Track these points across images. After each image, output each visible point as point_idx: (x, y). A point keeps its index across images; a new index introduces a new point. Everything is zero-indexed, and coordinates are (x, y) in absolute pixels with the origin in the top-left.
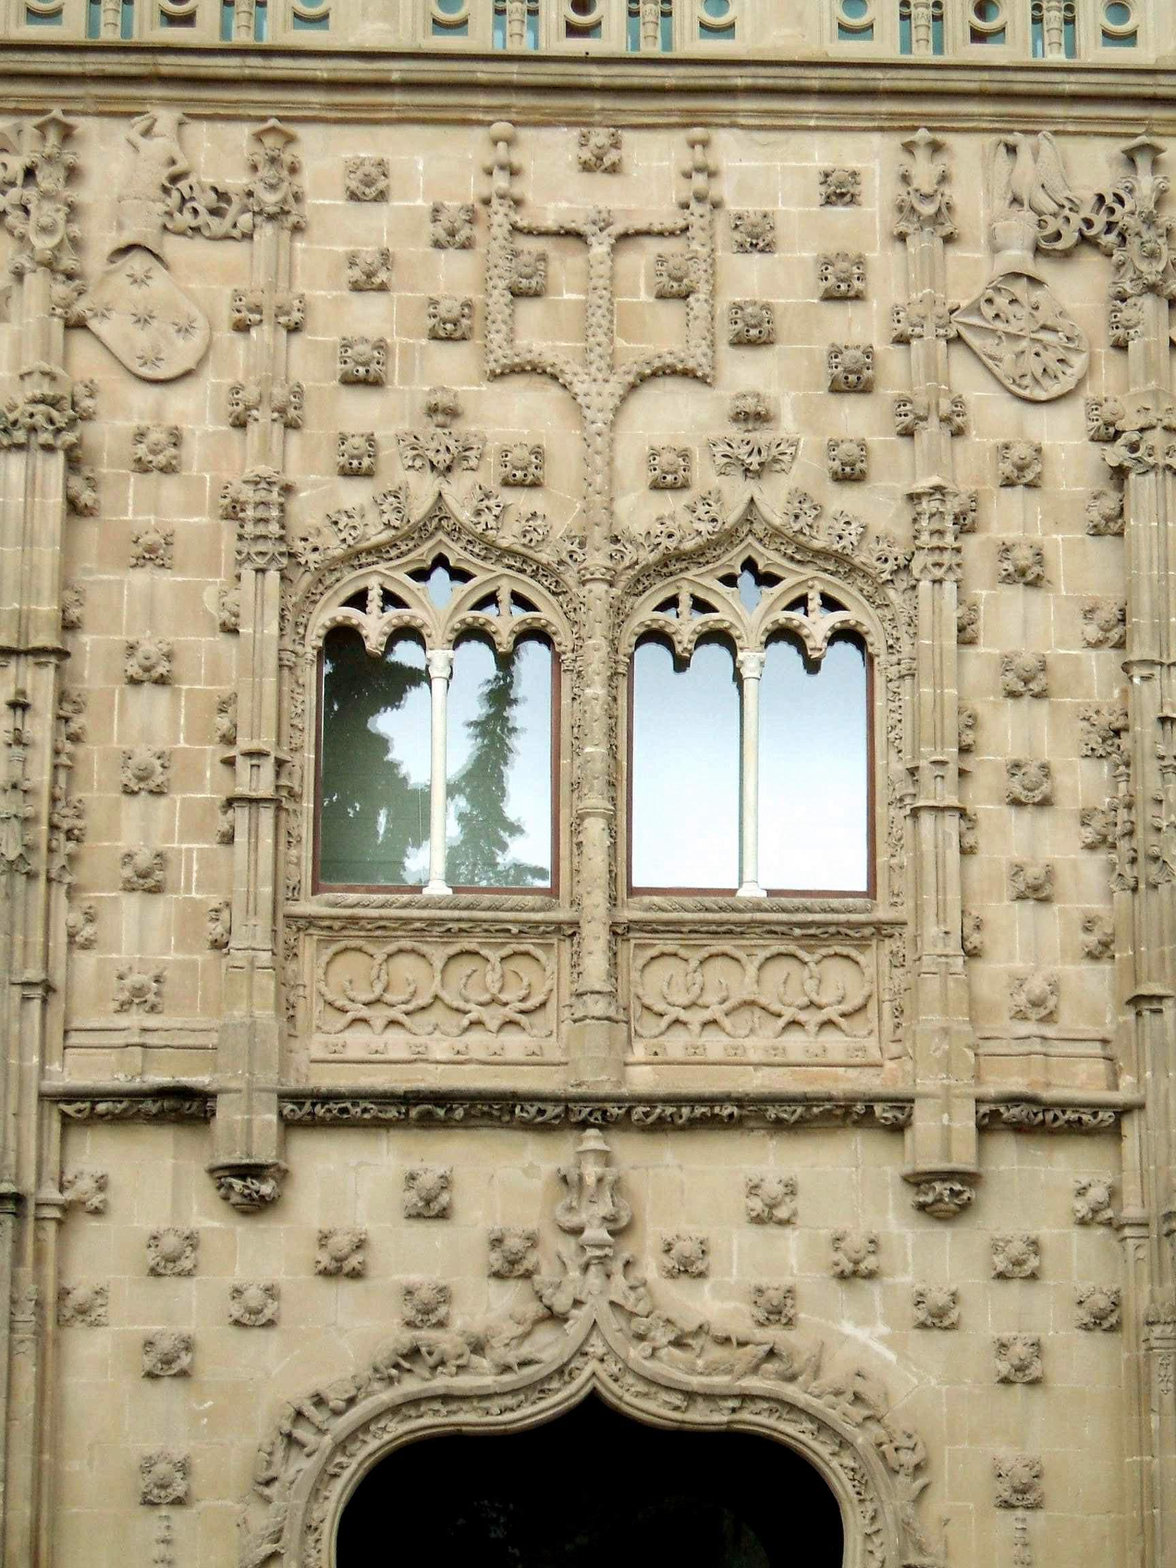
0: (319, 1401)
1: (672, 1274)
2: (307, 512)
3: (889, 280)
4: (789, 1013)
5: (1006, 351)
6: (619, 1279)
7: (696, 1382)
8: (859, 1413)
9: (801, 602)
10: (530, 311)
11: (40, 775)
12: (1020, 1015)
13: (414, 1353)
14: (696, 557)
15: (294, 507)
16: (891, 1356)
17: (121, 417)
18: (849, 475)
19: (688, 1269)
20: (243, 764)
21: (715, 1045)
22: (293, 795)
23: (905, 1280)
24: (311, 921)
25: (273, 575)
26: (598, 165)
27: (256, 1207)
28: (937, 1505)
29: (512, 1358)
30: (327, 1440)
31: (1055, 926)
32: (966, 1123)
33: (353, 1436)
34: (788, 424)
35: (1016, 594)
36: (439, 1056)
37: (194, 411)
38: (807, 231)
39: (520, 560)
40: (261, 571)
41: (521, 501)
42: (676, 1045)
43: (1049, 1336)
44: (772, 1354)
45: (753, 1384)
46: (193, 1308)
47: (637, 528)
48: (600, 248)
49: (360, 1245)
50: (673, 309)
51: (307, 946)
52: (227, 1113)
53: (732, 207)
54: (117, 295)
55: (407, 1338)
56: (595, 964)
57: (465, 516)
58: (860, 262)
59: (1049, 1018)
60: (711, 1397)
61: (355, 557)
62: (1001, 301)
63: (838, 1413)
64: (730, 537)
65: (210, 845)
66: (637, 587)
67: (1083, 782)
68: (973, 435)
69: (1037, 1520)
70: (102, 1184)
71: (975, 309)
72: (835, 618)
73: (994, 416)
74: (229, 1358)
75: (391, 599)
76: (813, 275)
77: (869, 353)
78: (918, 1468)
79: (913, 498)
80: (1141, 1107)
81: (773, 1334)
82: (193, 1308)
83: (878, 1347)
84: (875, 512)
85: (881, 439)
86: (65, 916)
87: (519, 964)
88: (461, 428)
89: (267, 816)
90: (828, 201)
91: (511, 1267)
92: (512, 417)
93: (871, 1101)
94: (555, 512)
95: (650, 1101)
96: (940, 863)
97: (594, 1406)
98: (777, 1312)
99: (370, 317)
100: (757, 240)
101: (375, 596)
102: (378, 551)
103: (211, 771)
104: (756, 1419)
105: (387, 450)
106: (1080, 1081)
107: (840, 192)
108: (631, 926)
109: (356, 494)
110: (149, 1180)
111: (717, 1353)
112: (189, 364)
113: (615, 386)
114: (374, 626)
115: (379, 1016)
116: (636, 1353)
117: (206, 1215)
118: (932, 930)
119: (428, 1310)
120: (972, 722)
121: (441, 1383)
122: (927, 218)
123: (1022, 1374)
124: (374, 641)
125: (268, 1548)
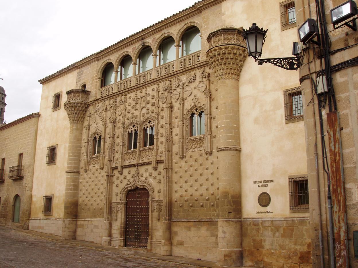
2: (126, 123)
3: (156, 97)
10: (137, 105)
11: (111, 146)
16: (152, 181)
17: (118, 118)
24: (125, 153)
26: (141, 92)
27: (121, 174)
28: (155, 193)
31: (163, 146)
34: (150, 110)
35: (162, 119)
37: (121, 117)
45: (144, 184)
48: (140, 99)
51: (126, 156)
54: (118, 110)
56: (137, 153)
59: (162, 153)
63: (148, 186)
64: (147, 119)
69: (160, 194)
70: (115, 173)
78: (153, 190)
85: (155, 109)
86: (113, 155)
92: (136, 113)
98: (146, 178)
99: (130, 108)
100: (149, 96)
104: (145, 187)
106: (163, 158)
107: (153, 90)
108: (141, 151)
112: (120, 114)
116: (137, 183)
117: (119, 175)
118: (154, 148)
119: (129, 181)
120: (159, 130)
122: (158, 91)
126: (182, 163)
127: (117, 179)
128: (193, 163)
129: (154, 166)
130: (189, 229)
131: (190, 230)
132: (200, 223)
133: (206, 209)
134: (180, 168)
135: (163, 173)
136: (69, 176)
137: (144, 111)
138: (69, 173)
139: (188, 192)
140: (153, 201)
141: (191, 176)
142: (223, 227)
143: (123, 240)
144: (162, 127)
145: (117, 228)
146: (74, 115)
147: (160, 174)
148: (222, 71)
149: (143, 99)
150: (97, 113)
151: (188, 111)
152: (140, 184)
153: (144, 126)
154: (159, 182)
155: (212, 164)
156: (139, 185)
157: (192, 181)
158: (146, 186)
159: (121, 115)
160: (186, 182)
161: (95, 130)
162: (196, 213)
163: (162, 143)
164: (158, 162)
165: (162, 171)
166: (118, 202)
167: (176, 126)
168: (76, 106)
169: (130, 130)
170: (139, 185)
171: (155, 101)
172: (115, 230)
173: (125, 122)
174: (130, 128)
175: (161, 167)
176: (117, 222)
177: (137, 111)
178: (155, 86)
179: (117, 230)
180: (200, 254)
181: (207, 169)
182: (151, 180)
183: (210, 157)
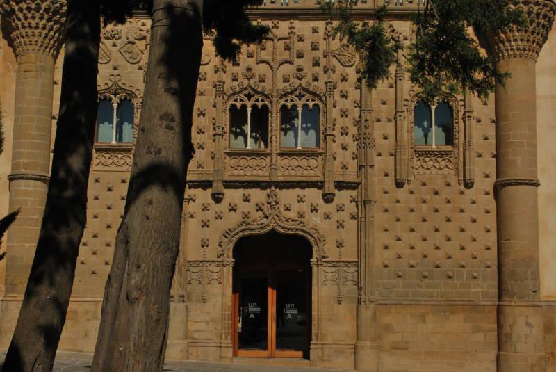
0: (230, 230)
1: (285, 210)
3: (322, 46)
4: (305, 168)
5: (342, 57)
6: (277, 211)
7: (289, 227)
8: (315, 231)
9: (308, 100)
12: (342, 168)
13: (244, 222)
14: (292, 93)
15: (225, 86)
18: (316, 79)
19: (288, 209)
20: (217, 129)
21: (293, 173)
22: (225, 133)
23: (323, 211)
25: (222, 97)
29: (259, 223)
30: (230, 236)
31: (348, 153)
32: (332, 186)
33: (235, 235)
34: (306, 70)
36: (249, 175)
38: (309, 38)
39: (262, 94)
40: (219, 96)
41: (263, 84)
42: (286, 173)
43: (345, 220)
44: (301, 222)
45: (298, 227)
46: (209, 215)
47: (281, 88)
48: (276, 41)
49: (236, 205)
50: (287, 52)
52: (215, 184)
53: (297, 33)
55: (243, 220)
57: (253, 86)
58: (318, 43)
60: (292, 230)
61: (235, 94)
62: (342, 49)
64: (296, 90)
65: (212, 141)
66: (281, 98)
67: (353, 130)
68: (337, 72)
69: (342, 249)
71: (337, 50)
72: (314, 102)
73: (339, 68)
74: (215, 223)
75: (241, 100)
76: (310, 45)
77: (319, 58)
78: (324, 241)
79: (326, 83)
80: (361, 183)
81: (302, 219)
82: (209, 215)
83: (319, 222)
84: (320, 86)
87: (262, 160)
88: (252, 72)
89: (220, 137)
90: (313, 33)
91: (260, 209)
93: (317, 182)
94: (267, 86)
95: (282, 182)
96: (330, 143)
97: (273, 230)
100: (301, 39)
101: (239, 100)
102: (239, 92)
103: (212, 129)
105: (240, 76)
106: (351, 178)
107: (315, 31)
109: (235, 83)
110: (203, 196)
111: (290, 222)
112: (207, 61)
113: (278, 64)
114: (239, 105)
115: (239, 168)
118: (328, 154)
121: (248, 227)
123: (340, 225)
124: (239, 107)
125: (221, 253)
126: (402, 194)
127: (205, 208)
128: (429, 197)
129: (331, 192)
130: (423, 318)
131: (424, 322)
132: (449, 307)
133: (458, 283)
134: (398, 201)
135: (351, 208)
136: (32, 189)
137: (287, 69)
138: (32, 181)
139: (417, 249)
140: (326, 262)
141: (424, 220)
142: (527, 317)
143: (231, 345)
144: (344, 114)
145: (207, 319)
146: (40, 30)
147: (340, 209)
148: (525, 43)
149: (282, 42)
150: (114, 40)
151: (416, 95)
152: (289, 225)
153: (282, 102)
154: (340, 225)
155: (474, 202)
156: (286, 227)
157: (425, 229)
158: (304, 232)
159: (208, 64)
160: (412, 230)
161: (110, 83)
162: (436, 290)
163: (344, 148)
164: (340, 186)
165: (346, 201)
166: (214, 261)
167: (384, 119)
168: (56, 12)
169: (239, 105)
170: (283, 228)
171: (322, 56)
172: (202, 323)
173: (224, 83)
174: (238, 97)
175: (343, 196)
176: (207, 304)
177: (264, 67)
178: (321, 24)
179: (207, 322)
180: (448, 364)
181: (462, 211)
182: (315, 220)
183: (467, 191)
